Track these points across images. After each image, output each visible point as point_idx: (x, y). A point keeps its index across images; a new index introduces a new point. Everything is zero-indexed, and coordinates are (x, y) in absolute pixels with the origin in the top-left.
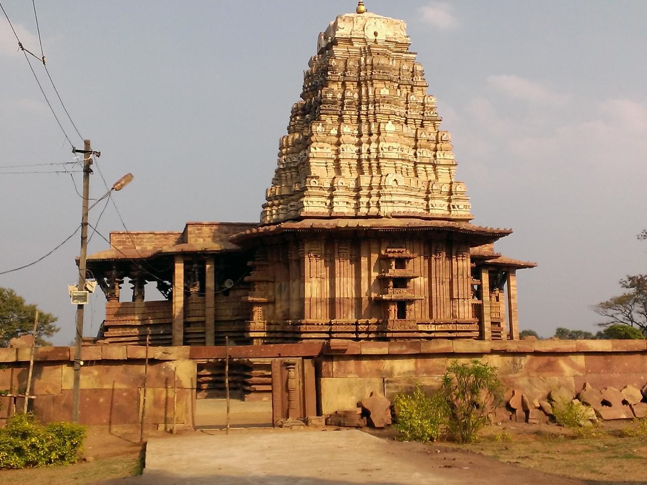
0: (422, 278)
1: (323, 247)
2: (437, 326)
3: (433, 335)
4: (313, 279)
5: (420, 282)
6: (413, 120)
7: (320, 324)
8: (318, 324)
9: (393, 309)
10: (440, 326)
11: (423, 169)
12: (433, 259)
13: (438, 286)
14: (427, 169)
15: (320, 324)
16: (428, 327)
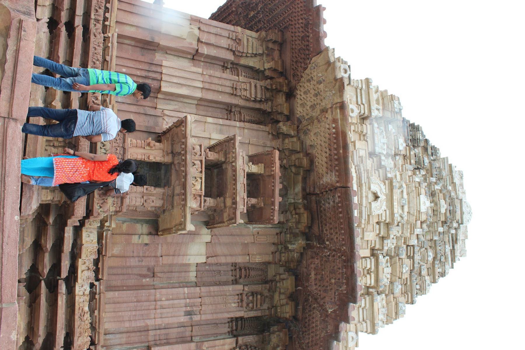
0: (203, 260)
1: (251, 64)
2: (88, 298)
3: (63, 288)
4: (197, 32)
5: (196, 250)
6: (412, 255)
7: (107, 15)
8: (107, 10)
9: (155, 154)
10: (86, 309)
11: (369, 267)
12: (240, 287)
13: (183, 301)
14: (368, 276)
15: (107, 15)
16: (89, 269)
